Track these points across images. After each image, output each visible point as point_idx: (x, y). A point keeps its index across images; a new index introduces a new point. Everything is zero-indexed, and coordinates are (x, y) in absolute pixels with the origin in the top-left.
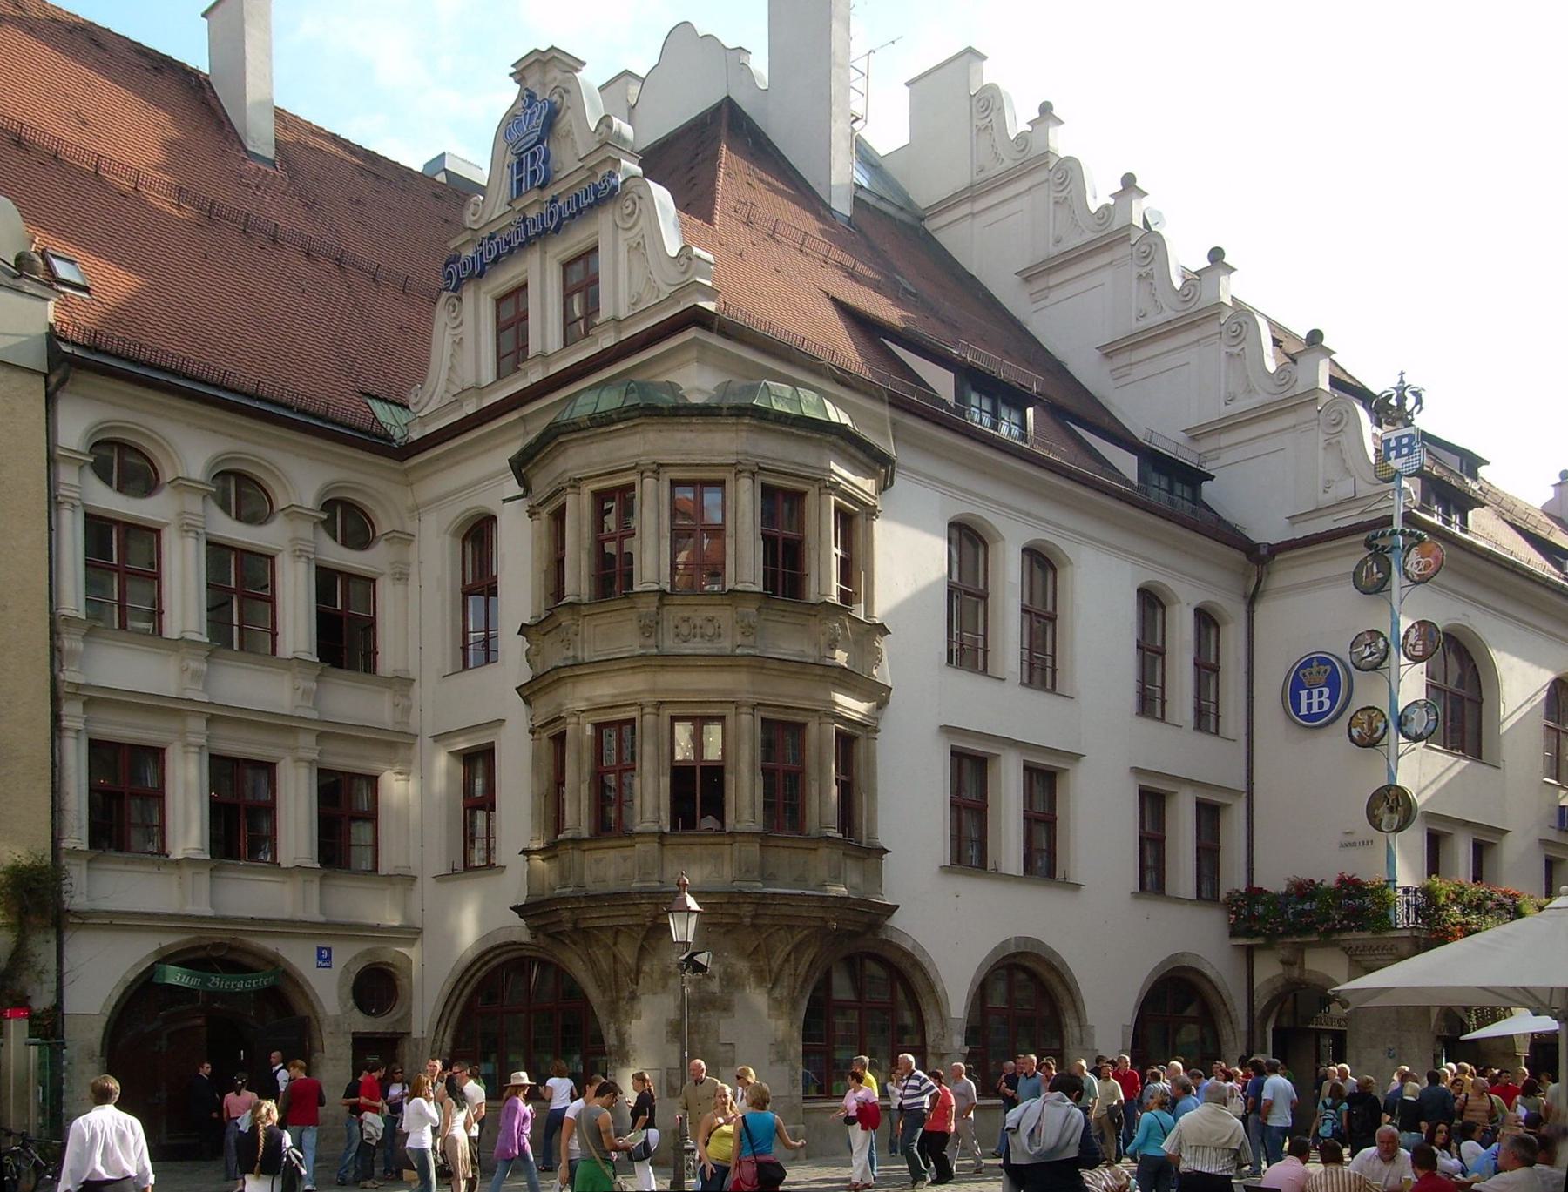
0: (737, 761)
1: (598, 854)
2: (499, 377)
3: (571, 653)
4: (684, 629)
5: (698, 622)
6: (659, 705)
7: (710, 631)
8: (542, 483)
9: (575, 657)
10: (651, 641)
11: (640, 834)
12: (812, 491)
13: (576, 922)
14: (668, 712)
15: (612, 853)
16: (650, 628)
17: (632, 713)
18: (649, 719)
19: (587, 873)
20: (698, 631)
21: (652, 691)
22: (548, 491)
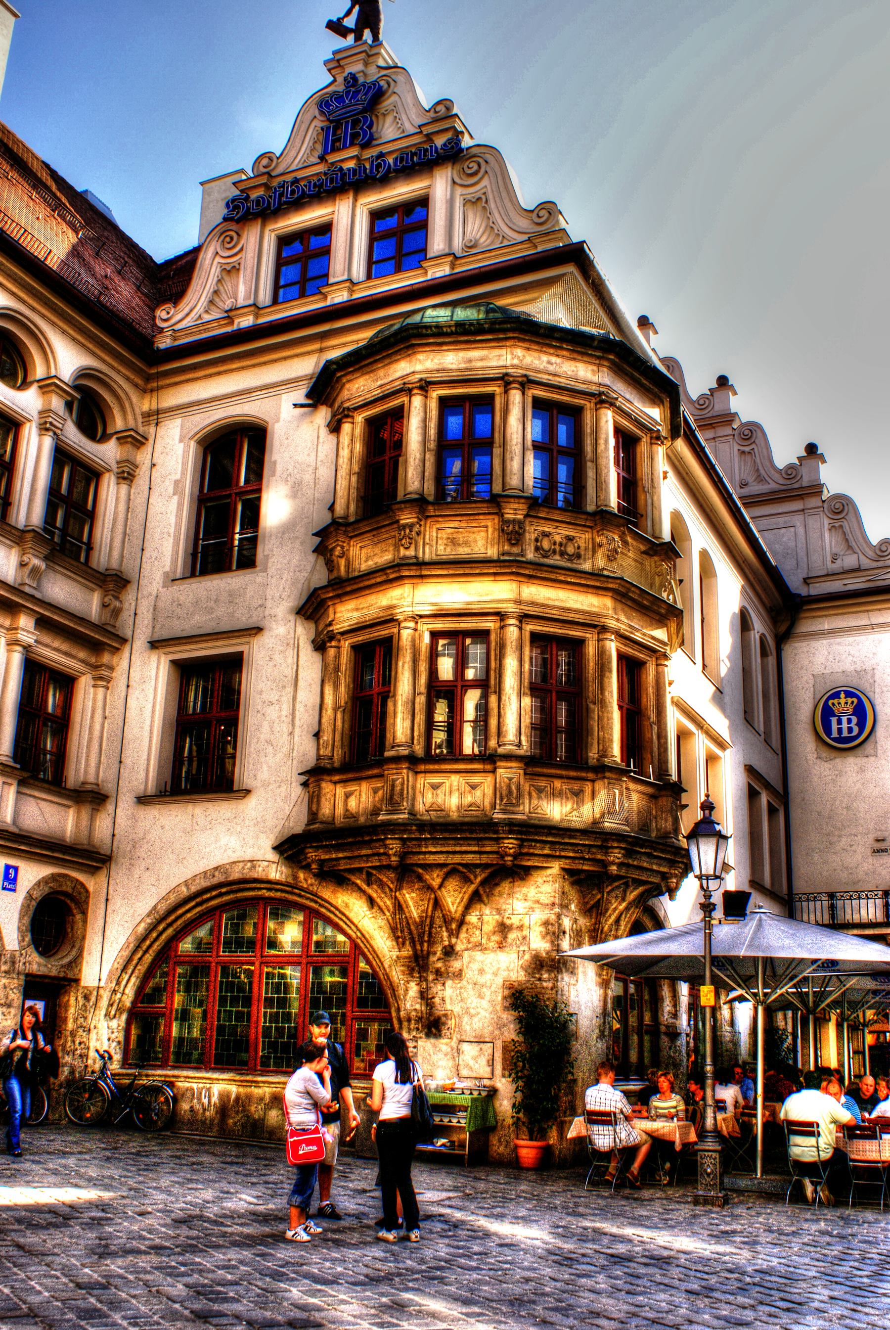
0: (602, 688)
1: (435, 779)
2: (275, 301)
3: (411, 552)
4: (546, 544)
5: (558, 538)
6: (523, 618)
7: (570, 550)
8: (360, 387)
9: (416, 557)
10: (515, 550)
11: (508, 757)
12: (645, 440)
13: (403, 856)
14: (529, 627)
15: (455, 779)
16: (512, 534)
17: (490, 624)
18: (512, 632)
19: (419, 799)
20: (557, 548)
21: (518, 602)
22: (377, 393)
